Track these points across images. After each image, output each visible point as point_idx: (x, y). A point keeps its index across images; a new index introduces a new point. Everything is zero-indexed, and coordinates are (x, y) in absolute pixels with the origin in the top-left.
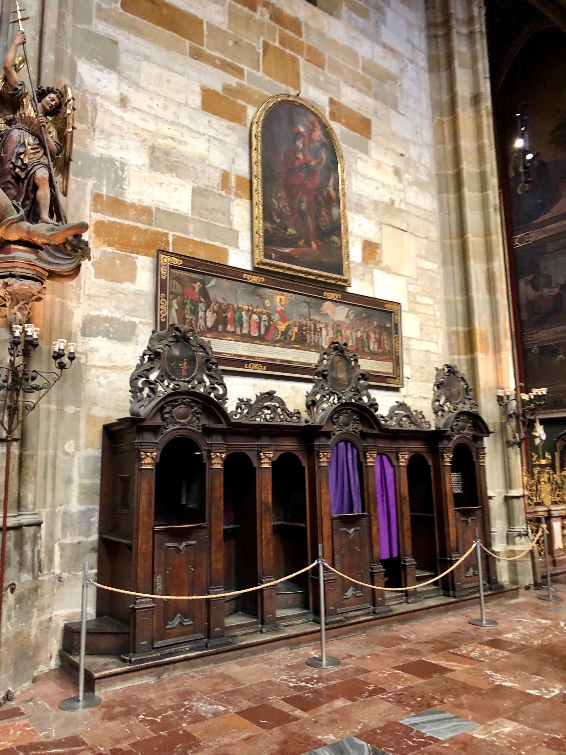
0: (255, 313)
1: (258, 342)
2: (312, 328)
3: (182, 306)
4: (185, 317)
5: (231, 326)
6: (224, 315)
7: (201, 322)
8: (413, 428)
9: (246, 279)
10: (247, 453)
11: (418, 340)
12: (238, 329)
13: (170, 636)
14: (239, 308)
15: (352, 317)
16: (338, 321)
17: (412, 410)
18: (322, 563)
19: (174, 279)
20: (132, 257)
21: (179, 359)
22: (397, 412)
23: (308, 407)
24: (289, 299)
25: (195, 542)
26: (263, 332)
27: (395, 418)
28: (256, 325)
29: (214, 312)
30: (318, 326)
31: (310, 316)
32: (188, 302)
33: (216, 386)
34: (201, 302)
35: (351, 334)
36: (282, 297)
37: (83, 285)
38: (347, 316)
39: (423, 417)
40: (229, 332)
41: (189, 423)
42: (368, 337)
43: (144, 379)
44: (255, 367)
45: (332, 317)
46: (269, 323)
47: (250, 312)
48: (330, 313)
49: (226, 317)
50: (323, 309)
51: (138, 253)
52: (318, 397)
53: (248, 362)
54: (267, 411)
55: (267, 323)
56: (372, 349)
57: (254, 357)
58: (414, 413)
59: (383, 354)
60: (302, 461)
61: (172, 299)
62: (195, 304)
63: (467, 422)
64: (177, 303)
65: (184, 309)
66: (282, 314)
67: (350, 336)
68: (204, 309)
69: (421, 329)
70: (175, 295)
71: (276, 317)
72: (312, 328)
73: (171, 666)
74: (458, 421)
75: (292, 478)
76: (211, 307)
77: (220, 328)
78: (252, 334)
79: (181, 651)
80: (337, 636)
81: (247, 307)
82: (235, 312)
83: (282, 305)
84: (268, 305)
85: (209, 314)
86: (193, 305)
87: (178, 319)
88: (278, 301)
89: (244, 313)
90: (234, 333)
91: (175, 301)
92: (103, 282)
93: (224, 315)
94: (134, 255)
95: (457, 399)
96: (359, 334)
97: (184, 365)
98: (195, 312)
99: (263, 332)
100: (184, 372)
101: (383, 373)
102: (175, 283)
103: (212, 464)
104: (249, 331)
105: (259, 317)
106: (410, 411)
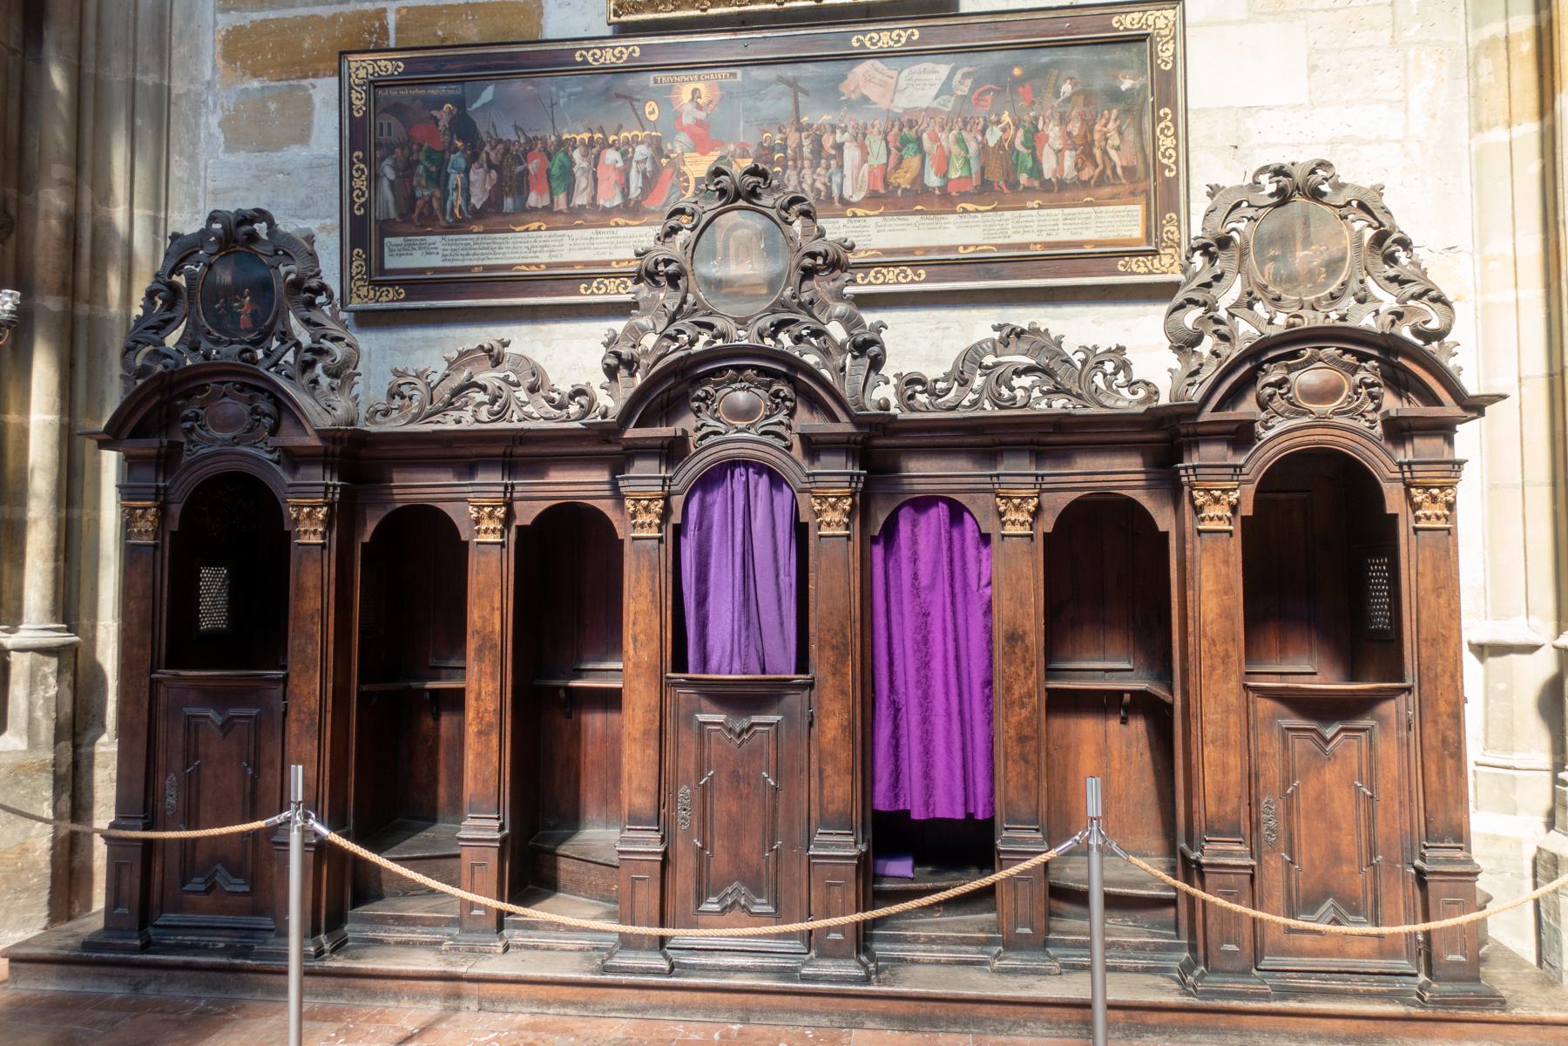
0: (610, 146)
1: (621, 221)
2: (806, 150)
3: (406, 170)
4: (413, 193)
5: (540, 193)
6: (520, 168)
7: (456, 199)
8: (1059, 404)
9: (585, 62)
10: (439, 505)
11: (1295, 107)
12: (561, 199)
13: (195, 908)
14: (561, 143)
15: (964, 90)
16: (906, 110)
17: (1068, 348)
18: (294, 815)
19: (384, 111)
20: (304, 89)
21: (235, 291)
22: (989, 360)
23: (611, 372)
24: (721, 87)
25: (254, 712)
26: (635, 192)
27: (978, 381)
28: (614, 176)
29: (491, 166)
30: (828, 141)
31: (798, 119)
32: (422, 156)
33: (327, 344)
34: (456, 150)
35: (961, 142)
36: (700, 86)
37: (202, 174)
38: (946, 88)
39: (1125, 366)
40: (534, 209)
41: (236, 441)
42: (1034, 137)
43: (151, 348)
44: (612, 287)
45: (883, 104)
46: (654, 162)
47: (594, 149)
48: (872, 92)
49: (527, 171)
50: (847, 88)
51: (315, 76)
52: (649, 341)
53: (589, 278)
54: (480, 397)
55: (648, 166)
56: (1048, 174)
57: (607, 263)
58: (1077, 359)
59: (1101, 181)
60: (616, 524)
61: (382, 160)
62: (440, 160)
63: (1354, 370)
64: (394, 167)
65: (410, 177)
66: (698, 130)
67: (955, 149)
68: (462, 163)
69: (1313, 68)
70: (390, 149)
71: (679, 144)
72: (806, 150)
73: (165, 974)
74: (1291, 369)
75: (567, 571)
76: (484, 156)
77: (509, 203)
78: (601, 202)
79: (206, 947)
80: (644, 1009)
81: (586, 136)
82: (550, 157)
83: (699, 107)
84: (653, 118)
85: (476, 175)
86: (432, 162)
87: (396, 204)
88: (685, 93)
89: (576, 155)
90: (549, 210)
91: (388, 161)
92: (242, 157)
93: (520, 168)
94: (305, 82)
95: (1325, 286)
96: (993, 137)
97: (245, 306)
98: (439, 179)
99: (635, 192)
100: (245, 321)
101: (1097, 244)
102: (388, 119)
103: (298, 535)
104: (594, 198)
105: (624, 155)
106: (1060, 353)
